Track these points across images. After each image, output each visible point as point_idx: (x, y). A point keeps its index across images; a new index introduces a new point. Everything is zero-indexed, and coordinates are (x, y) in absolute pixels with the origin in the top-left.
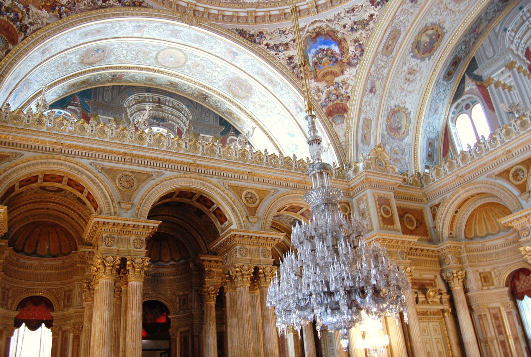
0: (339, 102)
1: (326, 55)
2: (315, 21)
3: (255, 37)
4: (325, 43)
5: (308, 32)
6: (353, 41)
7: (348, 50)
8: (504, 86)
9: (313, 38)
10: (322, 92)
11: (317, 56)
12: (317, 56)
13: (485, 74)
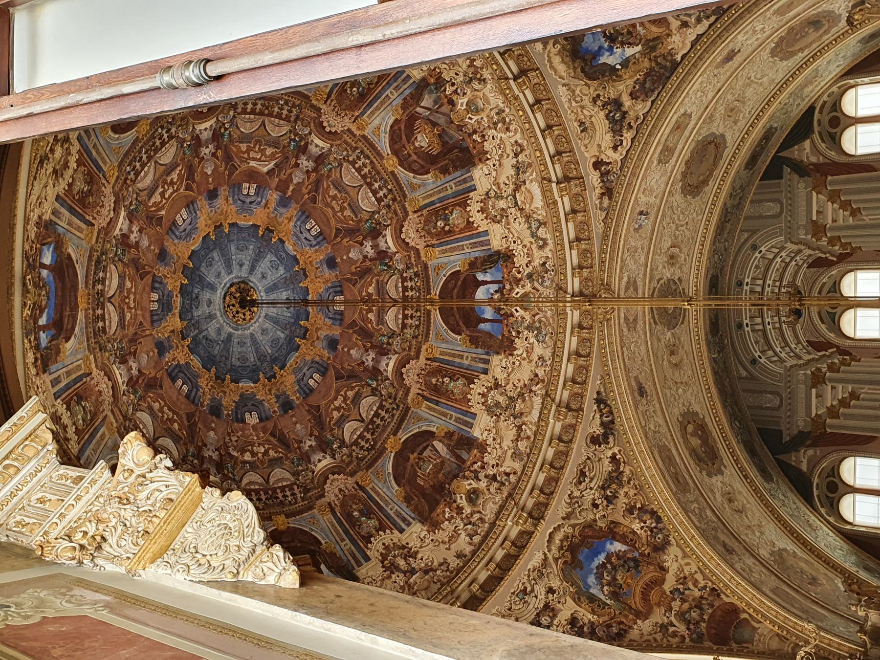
0: (710, 611)
1: (614, 568)
4: (597, 554)
5: (556, 560)
7: (634, 533)
8: (844, 403)
10: (672, 625)
11: (605, 581)
13: (801, 424)
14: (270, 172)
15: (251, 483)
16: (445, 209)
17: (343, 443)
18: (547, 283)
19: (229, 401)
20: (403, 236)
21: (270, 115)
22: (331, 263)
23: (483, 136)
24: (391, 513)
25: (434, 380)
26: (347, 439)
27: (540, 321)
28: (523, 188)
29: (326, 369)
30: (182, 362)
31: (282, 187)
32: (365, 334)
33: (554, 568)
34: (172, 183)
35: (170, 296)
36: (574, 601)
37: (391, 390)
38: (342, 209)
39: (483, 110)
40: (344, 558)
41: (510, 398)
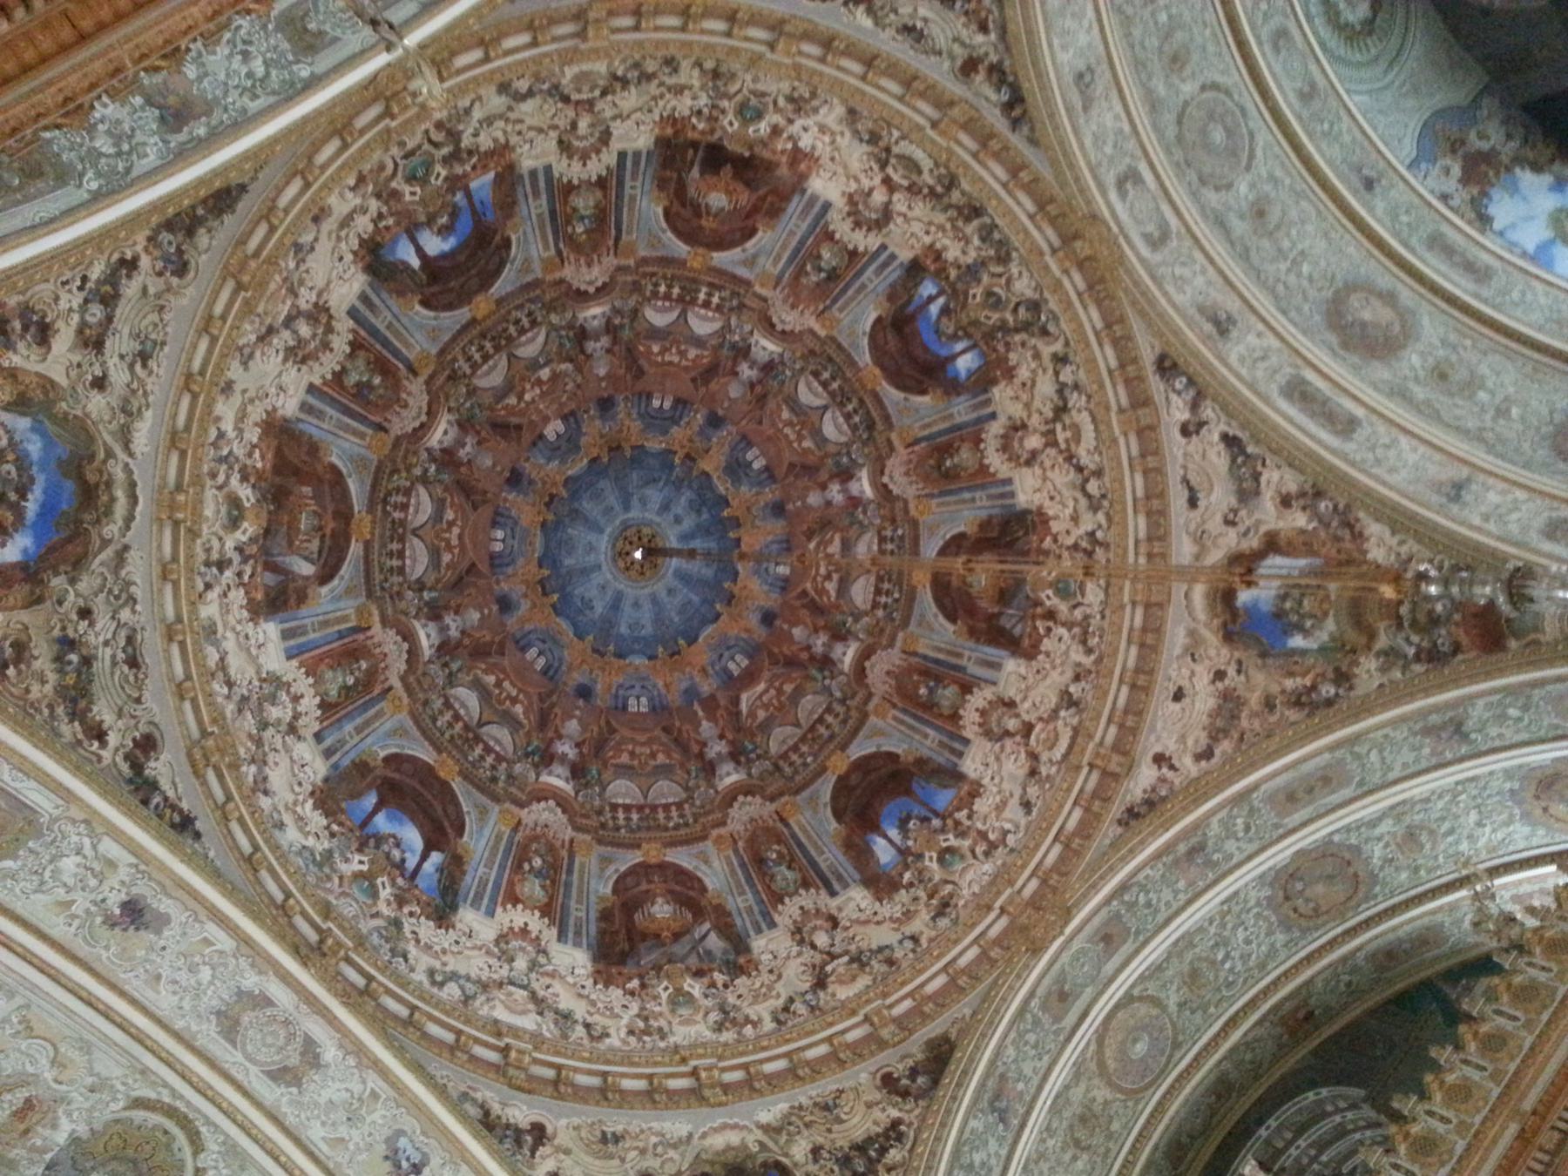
2: (133, 499)
3: (180, 237)
4: (47, 509)
5: (110, 454)
6: (24, 638)
9: (80, 466)
12: (11, 457)
14: (736, 701)
15: (533, 339)
16: (553, 882)
17: (424, 480)
18: (375, 939)
19: (594, 429)
20: (551, 803)
21: (803, 739)
22: (585, 692)
23: (632, 993)
24: (330, 411)
25: (364, 665)
26: (422, 490)
27: (329, 878)
28: (531, 1006)
29: (492, 566)
30: (675, 430)
31: (710, 704)
32: (480, 652)
33: (106, 437)
34: (828, 577)
35: (736, 481)
36: (52, 382)
37: (402, 605)
38: (632, 754)
39: (673, 1011)
40: (385, 295)
41: (264, 725)
